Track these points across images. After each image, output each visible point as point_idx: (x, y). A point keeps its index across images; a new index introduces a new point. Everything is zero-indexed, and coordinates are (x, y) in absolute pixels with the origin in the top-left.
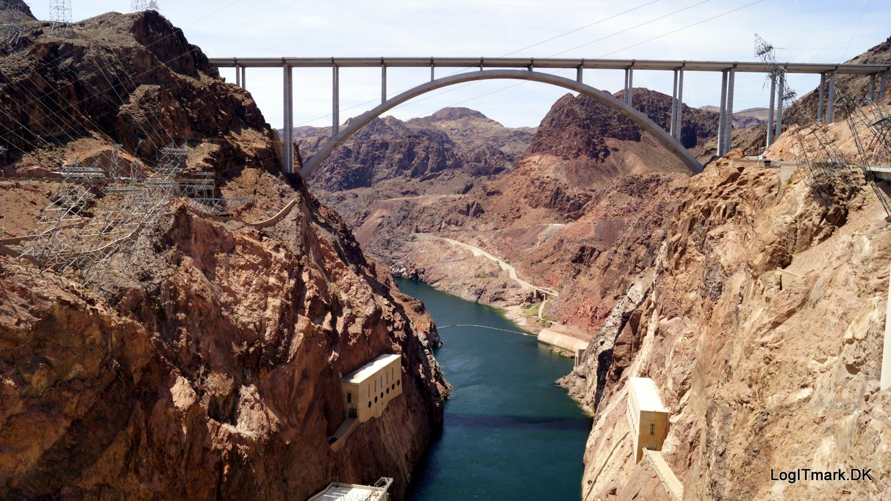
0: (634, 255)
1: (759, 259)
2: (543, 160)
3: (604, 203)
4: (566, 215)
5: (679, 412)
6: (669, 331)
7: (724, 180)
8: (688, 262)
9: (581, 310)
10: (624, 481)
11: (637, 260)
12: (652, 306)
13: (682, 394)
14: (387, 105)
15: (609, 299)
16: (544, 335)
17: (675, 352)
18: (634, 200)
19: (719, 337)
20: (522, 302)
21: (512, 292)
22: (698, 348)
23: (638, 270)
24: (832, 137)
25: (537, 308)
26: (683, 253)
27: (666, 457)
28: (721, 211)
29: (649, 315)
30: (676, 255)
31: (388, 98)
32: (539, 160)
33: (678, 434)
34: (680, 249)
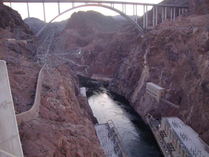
0: (113, 54)
1: (203, 49)
2: (71, 30)
3: (94, 41)
4: (81, 45)
5: (169, 88)
6: (156, 70)
7: (166, 32)
8: (159, 52)
9: (100, 70)
10: (156, 107)
11: (114, 55)
12: (144, 64)
13: (169, 84)
14: (60, 14)
15: (108, 66)
16: (92, 78)
17: (163, 74)
18: (102, 39)
19: (181, 69)
20: (79, 70)
21: (75, 68)
22: (171, 73)
23: (115, 57)
24: (188, 22)
25: (85, 71)
26: (156, 51)
27: (167, 99)
28: (168, 40)
29: (143, 67)
30: (154, 51)
31: (61, 13)
32: (70, 30)
33: (170, 93)
34: (155, 49)
